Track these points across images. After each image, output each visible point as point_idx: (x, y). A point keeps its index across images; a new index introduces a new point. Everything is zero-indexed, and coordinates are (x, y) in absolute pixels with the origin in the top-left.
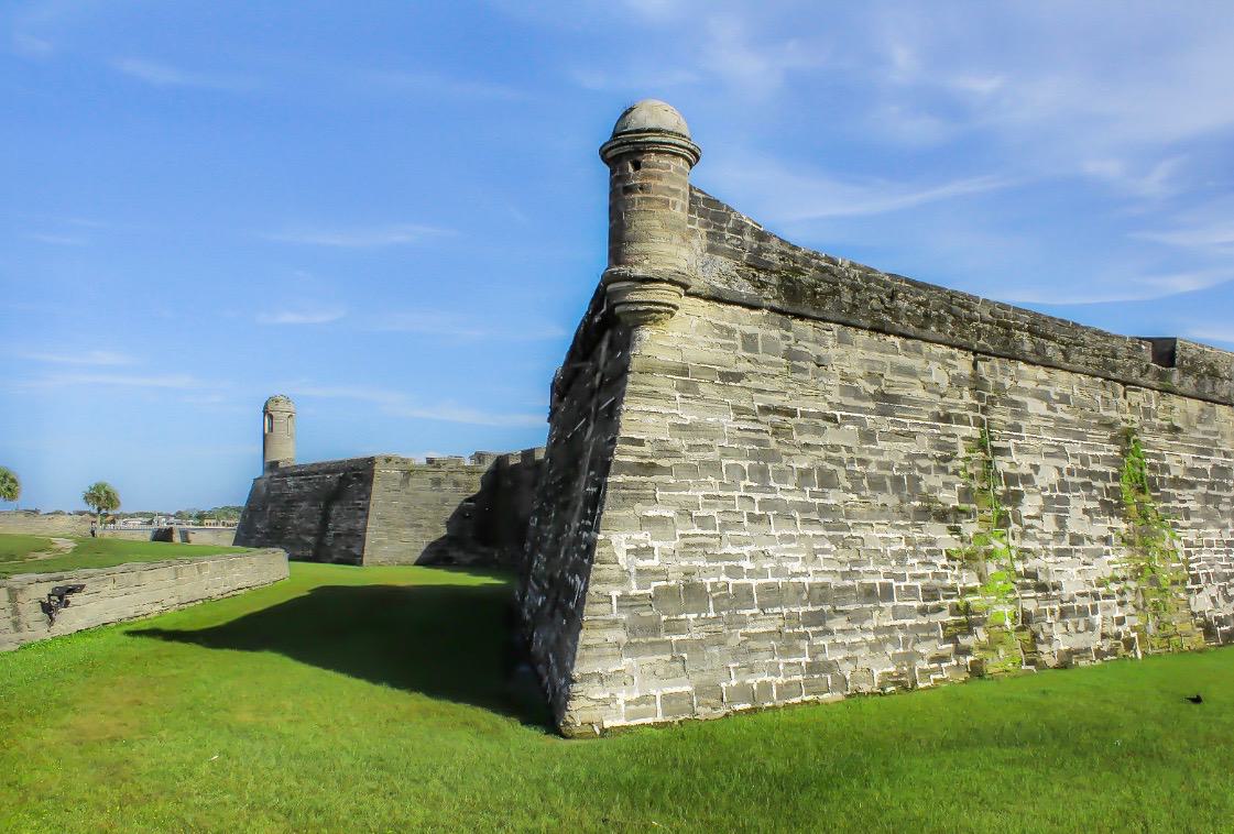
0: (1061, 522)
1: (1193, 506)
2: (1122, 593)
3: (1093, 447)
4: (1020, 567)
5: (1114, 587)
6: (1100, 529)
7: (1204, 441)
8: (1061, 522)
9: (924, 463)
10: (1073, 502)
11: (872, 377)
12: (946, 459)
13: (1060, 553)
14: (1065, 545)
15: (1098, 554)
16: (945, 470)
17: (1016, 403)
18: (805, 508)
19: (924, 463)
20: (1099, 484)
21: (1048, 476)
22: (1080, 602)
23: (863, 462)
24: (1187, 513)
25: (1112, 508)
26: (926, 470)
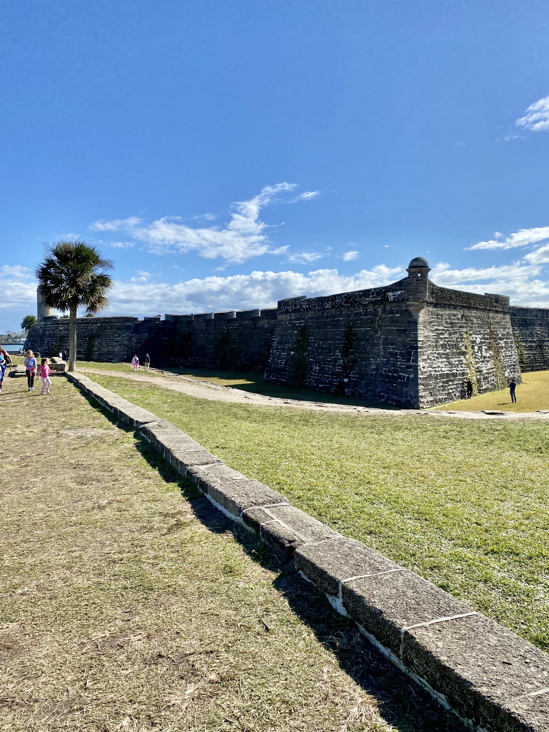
0: (481, 352)
1: (503, 345)
2: (493, 372)
3: (485, 331)
4: (476, 366)
5: (492, 371)
6: (488, 355)
7: (503, 325)
8: (481, 352)
9: (459, 340)
10: (483, 347)
11: (450, 318)
12: (462, 338)
13: (483, 362)
14: (483, 359)
15: (488, 361)
16: (462, 341)
17: (472, 320)
18: (443, 354)
19: (459, 340)
20: (487, 341)
21: (478, 341)
22: (487, 375)
23: (450, 341)
24: (502, 348)
25: (489, 348)
26: (459, 342)
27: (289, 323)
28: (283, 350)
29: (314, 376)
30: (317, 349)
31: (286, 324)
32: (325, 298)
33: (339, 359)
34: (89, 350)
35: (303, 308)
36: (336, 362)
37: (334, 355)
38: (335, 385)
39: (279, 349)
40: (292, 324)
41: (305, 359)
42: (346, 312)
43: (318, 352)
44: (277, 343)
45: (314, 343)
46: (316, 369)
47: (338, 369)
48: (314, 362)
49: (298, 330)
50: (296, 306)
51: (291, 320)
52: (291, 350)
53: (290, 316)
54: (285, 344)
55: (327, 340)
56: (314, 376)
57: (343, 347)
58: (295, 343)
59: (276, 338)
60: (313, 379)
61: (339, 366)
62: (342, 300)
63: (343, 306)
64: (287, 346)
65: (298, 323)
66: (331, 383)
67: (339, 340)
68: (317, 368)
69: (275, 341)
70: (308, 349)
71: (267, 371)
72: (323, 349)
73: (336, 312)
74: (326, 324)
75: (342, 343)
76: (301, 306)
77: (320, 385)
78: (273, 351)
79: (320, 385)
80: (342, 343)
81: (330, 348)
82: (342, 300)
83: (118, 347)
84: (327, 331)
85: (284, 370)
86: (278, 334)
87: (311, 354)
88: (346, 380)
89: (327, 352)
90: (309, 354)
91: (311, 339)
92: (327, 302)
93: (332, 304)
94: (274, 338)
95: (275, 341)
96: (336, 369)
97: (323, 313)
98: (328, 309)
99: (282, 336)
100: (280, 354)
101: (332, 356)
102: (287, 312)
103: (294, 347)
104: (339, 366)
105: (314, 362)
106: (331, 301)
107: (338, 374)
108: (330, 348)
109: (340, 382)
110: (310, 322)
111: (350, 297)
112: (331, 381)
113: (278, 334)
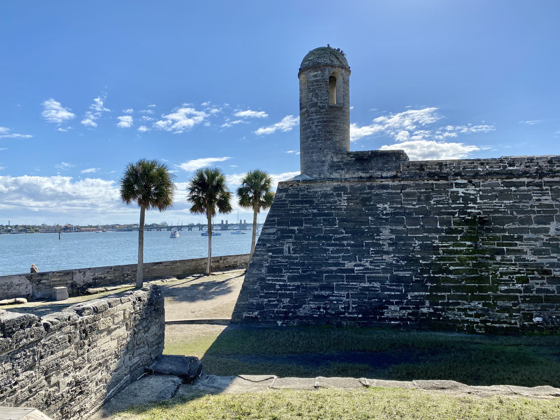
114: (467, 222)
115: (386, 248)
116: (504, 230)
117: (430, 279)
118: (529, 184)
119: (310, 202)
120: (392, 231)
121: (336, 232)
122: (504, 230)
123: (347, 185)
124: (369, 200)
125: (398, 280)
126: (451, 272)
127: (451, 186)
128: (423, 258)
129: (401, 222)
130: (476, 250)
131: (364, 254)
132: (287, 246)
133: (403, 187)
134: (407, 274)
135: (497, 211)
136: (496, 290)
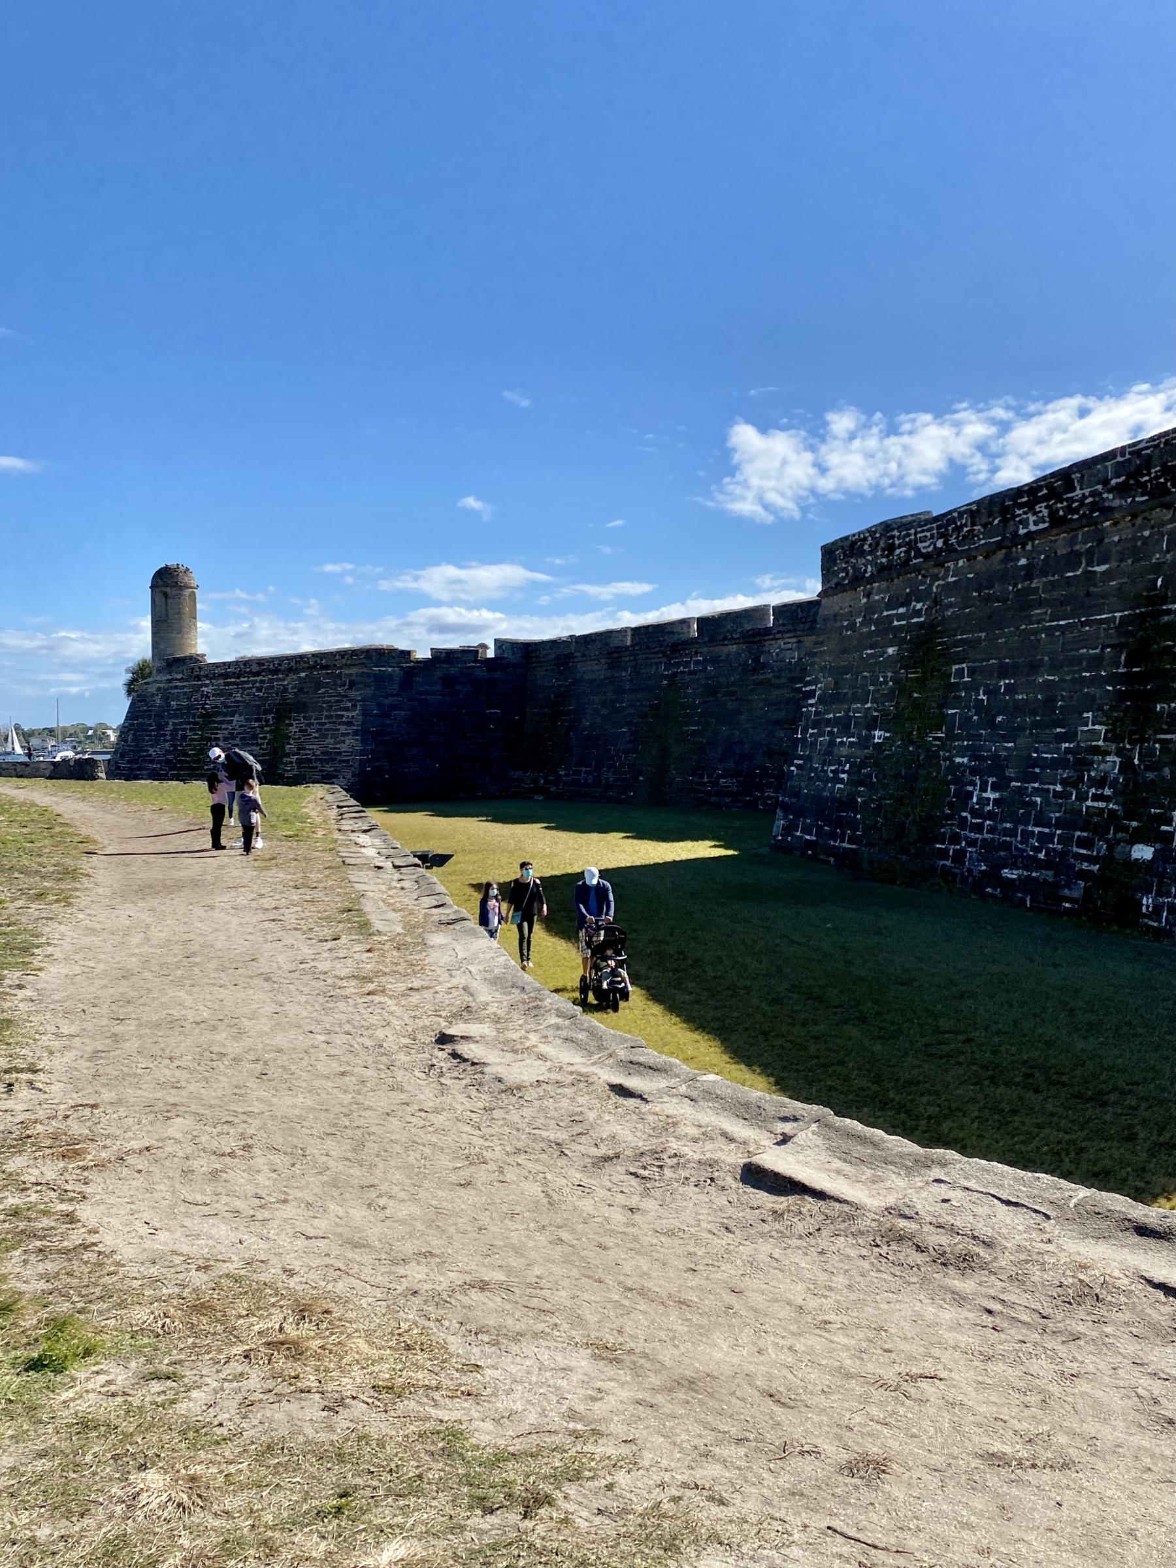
27: (867, 622)
28: (844, 726)
29: (978, 828)
30: (987, 715)
31: (852, 627)
32: (1018, 492)
33: (1096, 750)
34: (275, 752)
35: (919, 554)
36: (1083, 764)
37: (1069, 737)
38: (1083, 875)
39: (828, 722)
40: (877, 623)
41: (932, 757)
42: (1128, 533)
43: (992, 725)
44: (821, 700)
45: (972, 688)
46: (983, 802)
47: (1096, 798)
48: (974, 771)
49: (900, 643)
50: (891, 548)
51: (870, 609)
52: (872, 724)
53: (868, 595)
54: (855, 699)
55: (1034, 668)
56: (978, 828)
57: (1121, 696)
58: (890, 697)
59: (815, 682)
60: (971, 843)
61: (1101, 782)
62: (1106, 482)
63: (1107, 511)
64: (858, 710)
65: (900, 617)
66: (1060, 863)
67: (1095, 662)
68: (991, 795)
69: (811, 694)
70: (944, 716)
71: (786, 808)
72: (1018, 708)
73: (1073, 541)
74: (1025, 603)
75: (1114, 679)
76: (911, 546)
77: (1006, 872)
78: (805, 731)
79: (1006, 872)
80: (1114, 679)
81: (1050, 701)
82: (1106, 482)
83: (349, 741)
84: (1036, 632)
85: (849, 803)
86: (823, 669)
87: (959, 738)
88: (1143, 852)
89: (1036, 725)
90: (951, 736)
91: (960, 673)
92: (1030, 506)
93: (1053, 513)
94: (809, 683)
95: (811, 694)
96: (1082, 798)
97: (1008, 558)
98: (1030, 536)
99: (838, 673)
100: (832, 743)
101: (1061, 738)
102: (858, 579)
103: (885, 713)
104: (1101, 782)
105: (974, 771)
106: (1046, 498)
107: (1097, 825)
108: (1050, 701)
109: (1107, 861)
110: (951, 605)
111: (1148, 463)
112: (1063, 854)
113: (823, 669)
114: (202, 716)
115: (168, 738)
116: (215, 722)
117: (181, 762)
118: (234, 684)
119: (144, 701)
120: (174, 724)
121: (150, 725)
122: (215, 722)
123: (161, 685)
124: (168, 698)
125: (168, 761)
126: (188, 755)
127: (202, 686)
128: (181, 745)
129: (176, 716)
130: (202, 738)
131: (157, 742)
132: (130, 737)
133: (184, 687)
134: (170, 757)
135: (216, 707)
136: (202, 768)
